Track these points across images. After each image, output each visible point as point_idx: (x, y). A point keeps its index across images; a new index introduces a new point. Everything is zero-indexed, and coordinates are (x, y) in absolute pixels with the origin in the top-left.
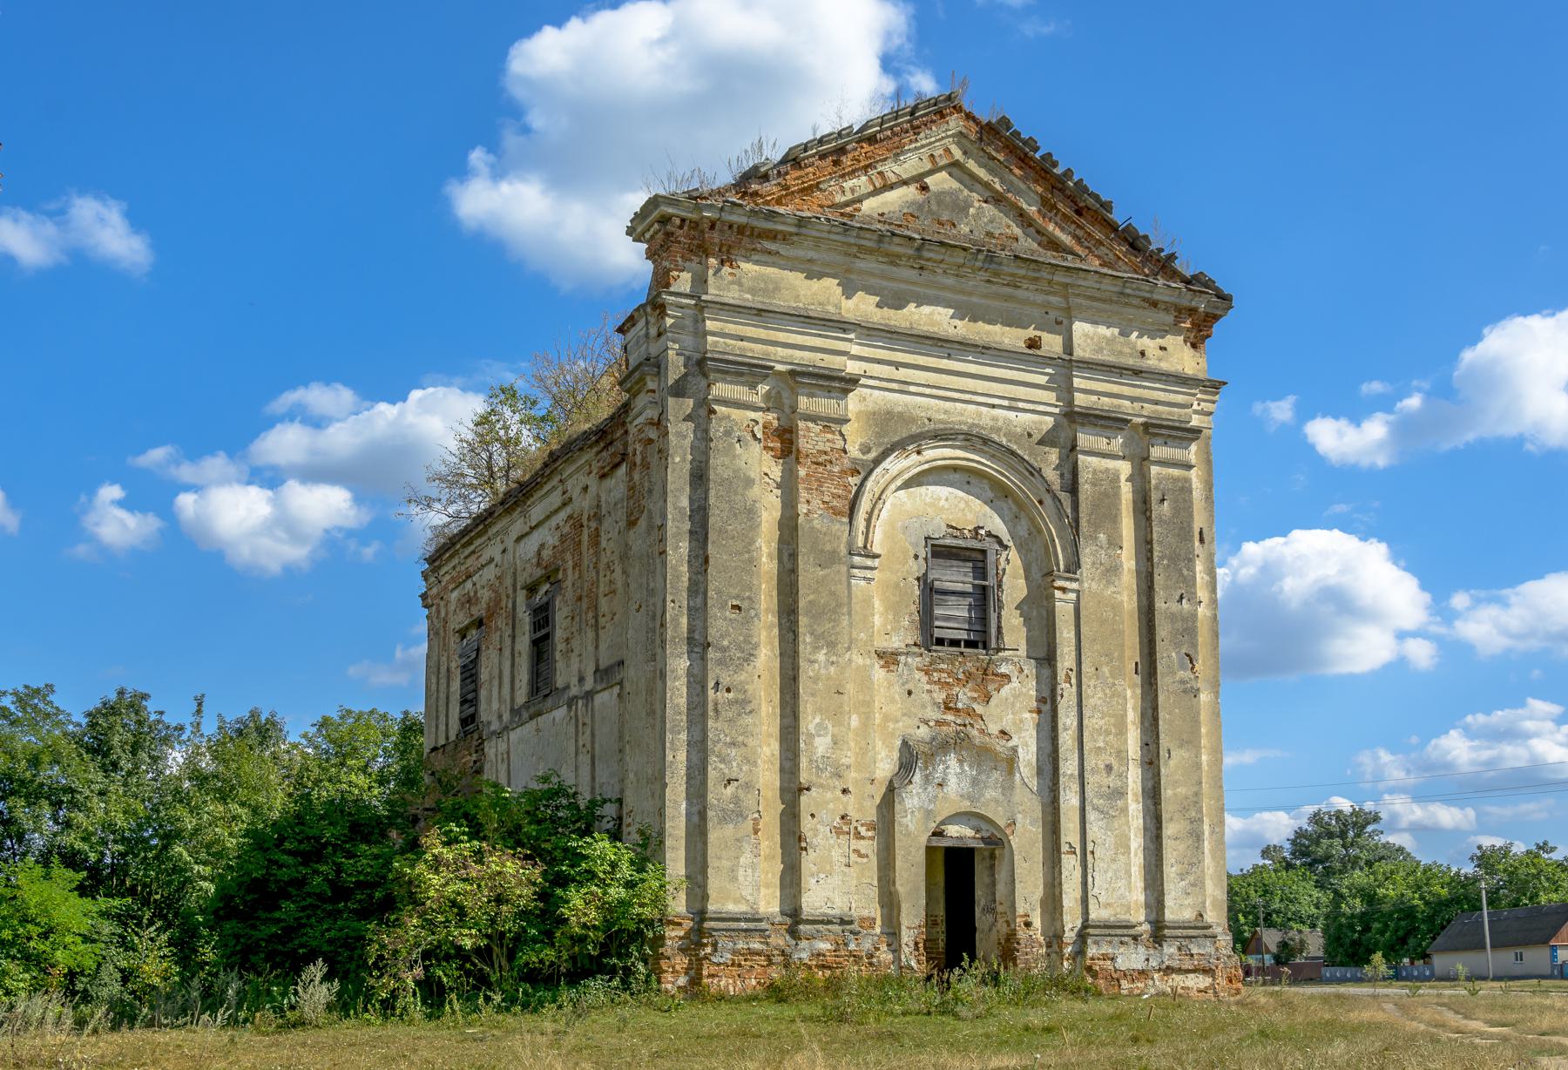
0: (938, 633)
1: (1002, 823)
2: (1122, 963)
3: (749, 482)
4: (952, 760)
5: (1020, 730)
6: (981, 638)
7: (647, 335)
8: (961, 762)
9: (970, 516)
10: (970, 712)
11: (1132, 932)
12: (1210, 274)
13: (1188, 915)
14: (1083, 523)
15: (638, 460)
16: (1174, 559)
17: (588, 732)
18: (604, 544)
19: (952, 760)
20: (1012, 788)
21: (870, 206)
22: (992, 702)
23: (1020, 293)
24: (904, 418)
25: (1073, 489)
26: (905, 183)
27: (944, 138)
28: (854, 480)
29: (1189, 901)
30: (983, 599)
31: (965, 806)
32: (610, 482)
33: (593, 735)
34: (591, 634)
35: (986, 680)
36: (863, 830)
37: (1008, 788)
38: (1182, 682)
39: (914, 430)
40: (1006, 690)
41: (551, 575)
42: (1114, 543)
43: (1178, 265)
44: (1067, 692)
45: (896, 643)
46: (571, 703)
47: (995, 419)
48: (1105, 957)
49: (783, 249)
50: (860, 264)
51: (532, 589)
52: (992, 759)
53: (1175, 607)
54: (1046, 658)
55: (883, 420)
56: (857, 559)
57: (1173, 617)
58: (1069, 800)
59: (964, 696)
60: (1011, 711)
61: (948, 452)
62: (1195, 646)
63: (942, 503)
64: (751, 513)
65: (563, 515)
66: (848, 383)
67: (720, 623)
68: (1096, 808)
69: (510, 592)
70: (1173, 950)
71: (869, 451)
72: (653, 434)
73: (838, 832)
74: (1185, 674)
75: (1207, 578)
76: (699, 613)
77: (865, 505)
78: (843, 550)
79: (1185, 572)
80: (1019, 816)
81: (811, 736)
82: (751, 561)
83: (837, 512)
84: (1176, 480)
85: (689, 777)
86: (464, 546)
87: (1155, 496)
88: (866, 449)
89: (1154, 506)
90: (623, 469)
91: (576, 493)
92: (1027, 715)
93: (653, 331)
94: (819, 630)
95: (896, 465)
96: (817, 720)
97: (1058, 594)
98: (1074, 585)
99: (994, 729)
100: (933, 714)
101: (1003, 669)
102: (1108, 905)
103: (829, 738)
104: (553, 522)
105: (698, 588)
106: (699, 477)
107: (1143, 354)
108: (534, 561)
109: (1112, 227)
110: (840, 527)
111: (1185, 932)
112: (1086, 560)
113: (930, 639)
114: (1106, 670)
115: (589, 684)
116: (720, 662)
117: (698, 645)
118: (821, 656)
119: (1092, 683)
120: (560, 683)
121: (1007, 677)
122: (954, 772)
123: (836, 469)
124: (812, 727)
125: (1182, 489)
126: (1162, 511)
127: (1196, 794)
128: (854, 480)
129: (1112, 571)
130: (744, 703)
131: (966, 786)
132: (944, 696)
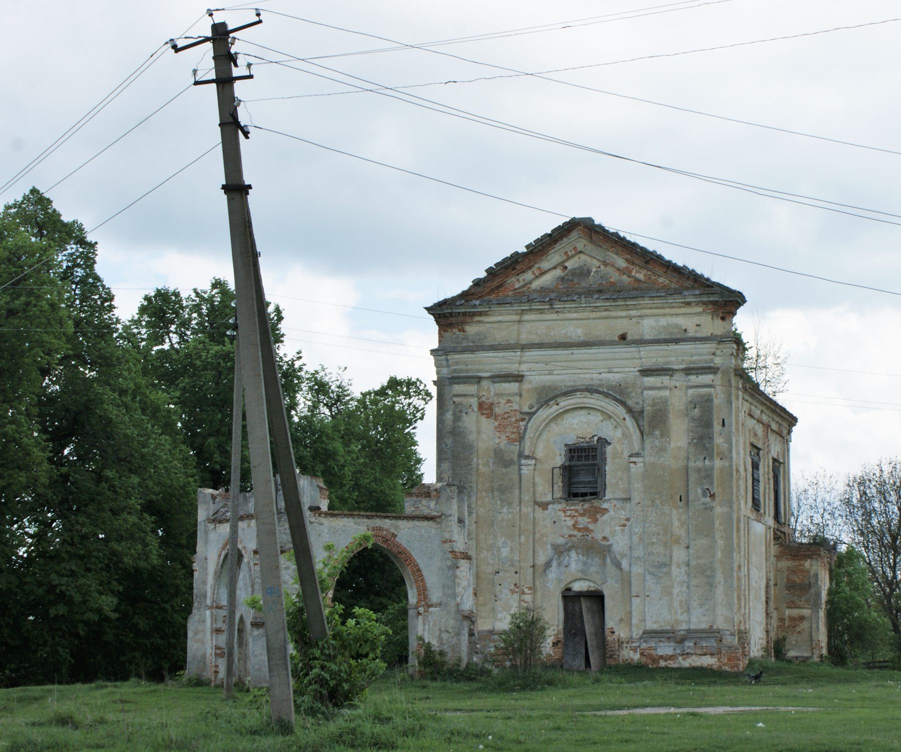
0: (574, 491)
1: (599, 583)
2: (660, 652)
4: (573, 554)
5: (614, 536)
8: (577, 553)
9: (589, 431)
10: (586, 529)
11: (667, 635)
13: (704, 626)
14: (646, 427)
19: (573, 554)
20: (604, 564)
21: (536, 284)
22: (599, 523)
23: (613, 314)
24: (551, 388)
26: (555, 268)
28: (524, 423)
29: (705, 619)
31: (580, 575)
35: (595, 514)
36: (526, 590)
38: (704, 504)
39: (557, 392)
40: (606, 517)
42: (665, 434)
45: (549, 498)
47: (601, 380)
48: (651, 648)
49: (485, 319)
50: (526, 317)
52: (597, 550)
53: (700, 464)
56: (523, 461)
57: (699, 470)
59: (583, 521)
62: (712, 484)
63: (575, 426)
66: (518, 378)
68: (650, 573)
70: (691, 644)
71: (533, 407)
73: (513, 592)
77: (529, 434)
78: (515, 458)
79: (707, 445)
80: (609, 579)
81: (499, 548)
83: (515, 440)
84: (702, 396)
88: (531, 407)
92: (618, 528)
94: (504, 498)
95: (545, 413)
96: (503, 539)
98: (641, 459)
99: (599, 536)
100: (567, 532)
101: (605, 506)
102: (655, 622)
103: (508, 549)
107: (686, 330)
110: (515, 448)
111: (699, 635)
114: (658, 502)
118: (505, 510)
119: (650, 509)
121: (606, 510)
122: (574, 561)
123: (513, 419)
124: (500, 544)
125: (707, 401)
127: (712, 563)
129: (662, 450)
131: (580, 566)
132: (573, 522)
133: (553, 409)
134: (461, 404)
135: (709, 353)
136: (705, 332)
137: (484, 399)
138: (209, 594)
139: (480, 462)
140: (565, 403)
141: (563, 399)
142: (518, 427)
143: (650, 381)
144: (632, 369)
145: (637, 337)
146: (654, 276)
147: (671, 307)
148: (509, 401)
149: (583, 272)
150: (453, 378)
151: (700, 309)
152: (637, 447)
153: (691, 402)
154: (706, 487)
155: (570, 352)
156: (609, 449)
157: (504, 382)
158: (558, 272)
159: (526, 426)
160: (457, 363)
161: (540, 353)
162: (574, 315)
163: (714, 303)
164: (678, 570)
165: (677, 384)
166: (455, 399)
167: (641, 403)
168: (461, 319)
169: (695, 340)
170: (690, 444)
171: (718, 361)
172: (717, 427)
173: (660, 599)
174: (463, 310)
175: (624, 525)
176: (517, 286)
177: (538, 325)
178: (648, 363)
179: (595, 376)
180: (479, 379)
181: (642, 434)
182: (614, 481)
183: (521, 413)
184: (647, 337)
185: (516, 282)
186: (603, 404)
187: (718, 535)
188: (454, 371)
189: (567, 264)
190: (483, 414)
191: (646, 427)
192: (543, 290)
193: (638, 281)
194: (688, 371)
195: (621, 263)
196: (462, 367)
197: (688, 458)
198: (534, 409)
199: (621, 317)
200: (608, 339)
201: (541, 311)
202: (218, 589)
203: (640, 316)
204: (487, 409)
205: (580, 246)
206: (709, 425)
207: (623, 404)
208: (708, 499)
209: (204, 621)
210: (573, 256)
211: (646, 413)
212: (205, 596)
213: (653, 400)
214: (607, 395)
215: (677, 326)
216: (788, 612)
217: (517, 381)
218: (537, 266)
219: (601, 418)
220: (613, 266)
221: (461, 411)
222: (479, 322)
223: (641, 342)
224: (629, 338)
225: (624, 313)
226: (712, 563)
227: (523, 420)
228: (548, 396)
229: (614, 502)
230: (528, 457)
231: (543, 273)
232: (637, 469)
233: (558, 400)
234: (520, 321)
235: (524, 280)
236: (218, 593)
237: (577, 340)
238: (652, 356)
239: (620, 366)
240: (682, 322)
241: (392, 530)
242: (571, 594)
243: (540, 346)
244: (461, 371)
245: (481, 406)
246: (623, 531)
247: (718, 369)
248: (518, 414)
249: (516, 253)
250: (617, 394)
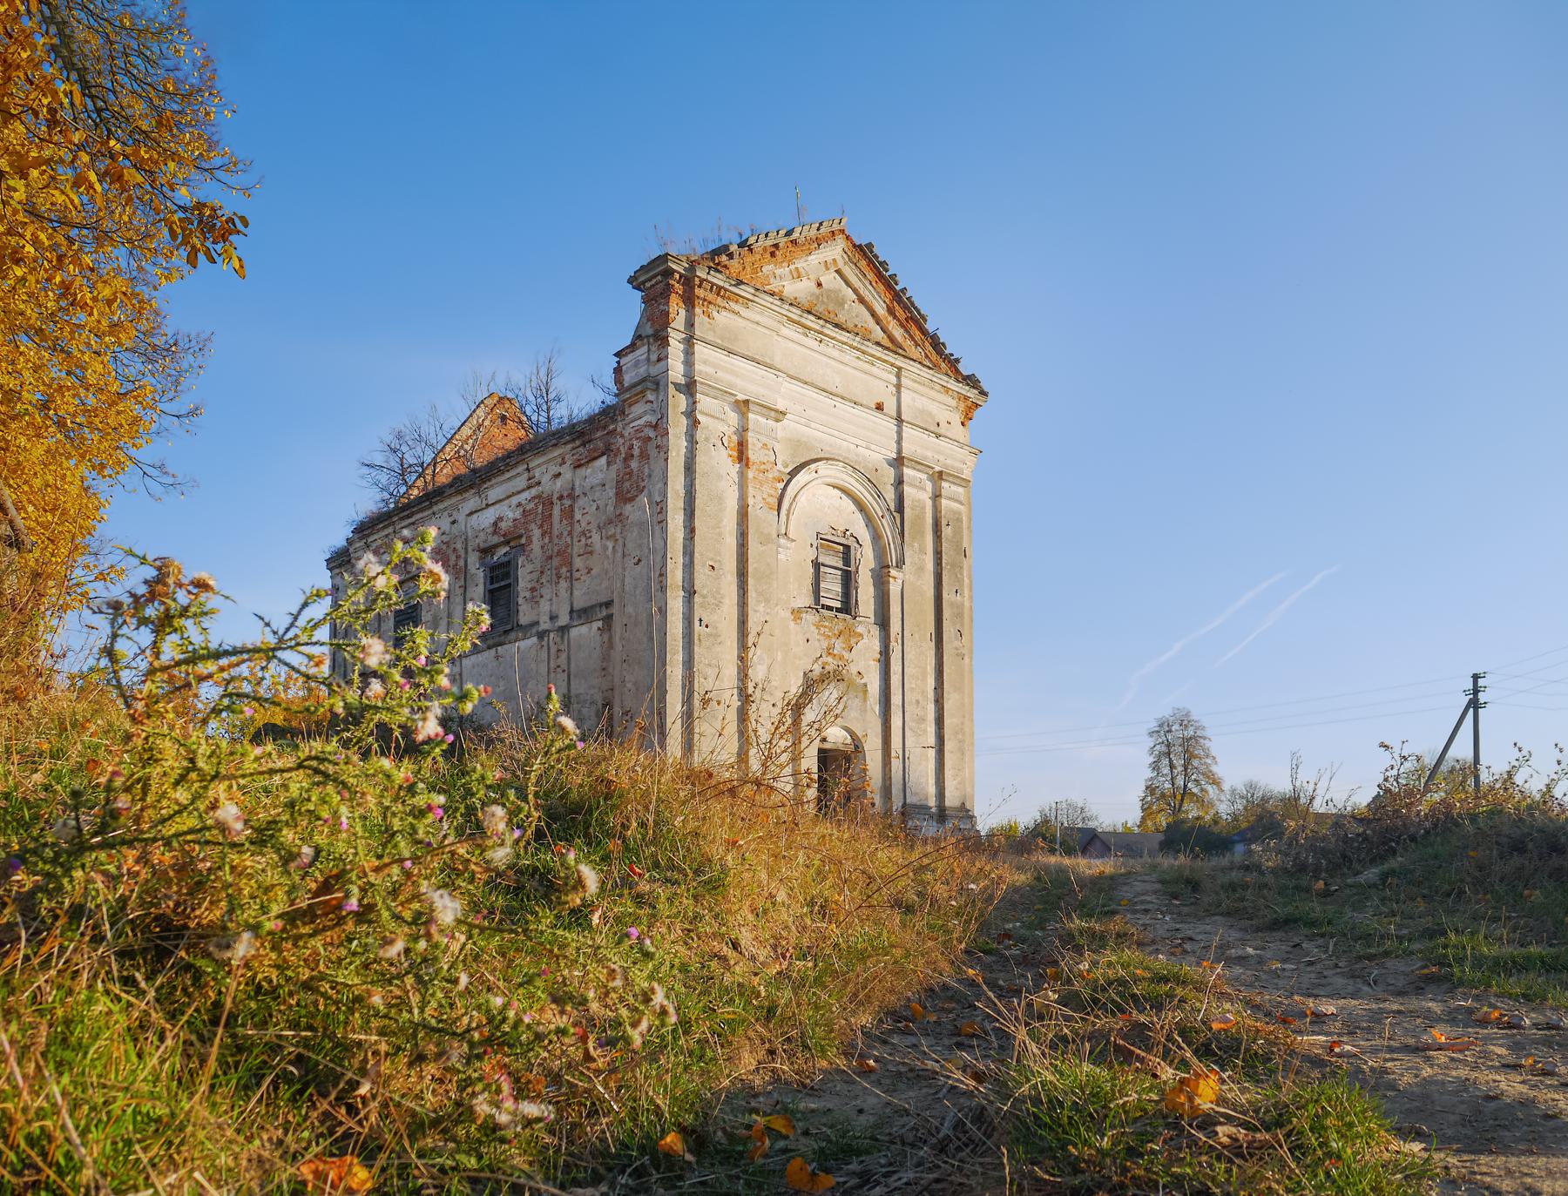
0: (823, 601)
6: (847, 606)
7: (648, 359)
12: (979, 377)
15: (636, 452)
16: (953, 565)
17: (564, 656)
18: (578, 516)
23: (874, 370)
25: (900, 508)
27: (835, 251)
30: (848, 580)
32: (582, 472)
33: (569, 658)
34: (563, 584)
35: (849, 635)
37: (864, 711)
41: (514, 539)
42: (922, 551)
43: (960, 367)
44: (895, 647)
46: (541, 635)
51: (486, 551)
54: (883, 622)
55: (797, 444)
58: (896, 722)
60: (864, 658)
64: (720, 499)
65: (526, 495)
66: (780, 415)
67: (701, 577)
69: (462, 553)
72: (652, 434)
74: (957, 644)
76: (689, 567)
82: (720, 534)
84: (955, 512)
85: (684, 687)
86: (402, 519)
87: (944, 522)
89: (944, 528)
90: (603, 460)
91: (545, 479)
93: (654, 357)
101: (860, 629)
104: (515, 500)
105: (689, 552)
106: (690, 468)
108: (490, 530)
109: (924, 332)
113: (818, 604)
115: (564, 620)
116: (702, 605)
117: (690, 592)
118: (761, 608)
120: (524, 619)
121: (861, 635)
126: (947, 532)
128: (781, 485)
130: (717, 636)
151: (954, 403)
157: (763, 415)
163: (966, 398)
168: (711, 297)
174: (721, 283)
195: (881, 310)
205: (840, 264)
215: (930, 414)
242: (827, 746)
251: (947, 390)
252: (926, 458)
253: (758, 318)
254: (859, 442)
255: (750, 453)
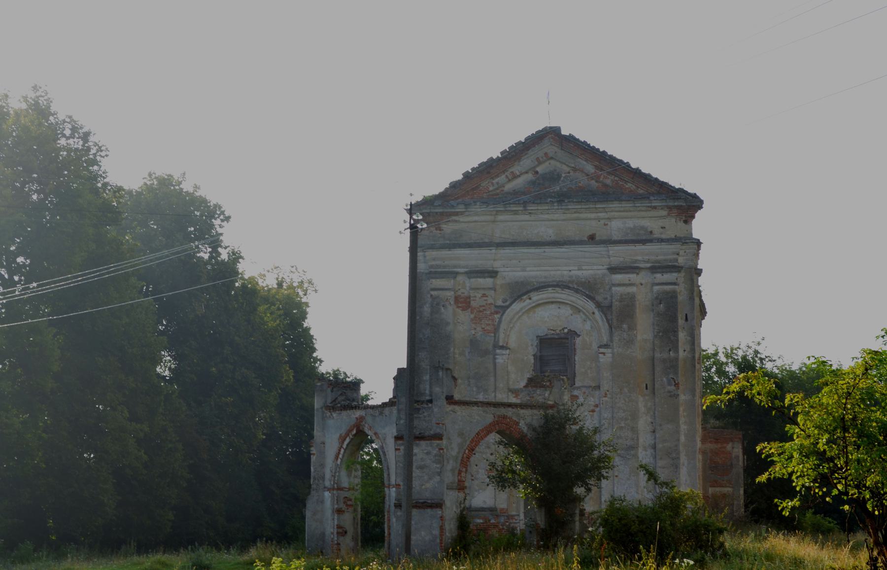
3: (448, 324)
14: (615, 321)
21: (509, 187)
26: (527, 172)
28: (497, 316)
38: (669, 392)
42: (632, 328)
47: (571, 277)
53: (665, 355)
56: (498, 351)
61: (544, 296)
62: (676, 373)
66: (493, 274)
75: (689, 338)
77: (503, 326)
78: (491, 348)
79: (672, 338)
84: (667, 293)
88: (505, 301)
95: (516, 306)
97: (601, 355)
98: (610, 350)
107: (651, 232)
112: (616, 339)
123: (488, 312)
127: (676, 446)
129: (630, 342)
133: (525, 304)
134: (438, 297)
135: (674, 253)
136: (670, 234)
137: (459, 293)
138: (328, 475)
139: (457, 351)
140: (536, 297)
141: (536, 293)
142: (493, 320)
143: (618, 277)
144: (601, 267)
145: (605, 238)
146: (619, 182)
147: (639, 211)
148: (484, 295)
149: (554, 177)
150: (430, 273)
152: (605, 339)
153: (657, 298)
154: (671, 376)
155: (542, 250)
156: (578, 341)
157: (480, 277)
158: (530, 176)
159: (500, 319)
160: (434, 259)
161: (512, 251)
162: (546, 216)
163: (679, 208)
164: (644, 453)
165: (643, 282)
166: (433, 293)
167: (609, 298)
169: (661, 241)
170: (655, 336)
171: (681, 261)
172: (681, 322)
173: (628, 479)
174: (441, 210)
175: (593, 411)
176: (491, 188)
177: (510, 224)
178: (615, 261)
179: (565, 273)
180: (455, 275)
181: (611, 327)
182: (583, 370)
183: (496, 306)
184: (615, 238)
185: (489, 185)
186: (573, 299)
187: (682, 420)
188: (432, 267)
189: (538, 169)
190: (458, 307)
191: (615, 321)
192: (515, 193)
193: (606, 185)
194: (656, 268)
195: (590, 168)
196: (438, 263)
197: (654, 350)
198: (508, 303)
199: (590, 219)
200: (577, 239)
201: (516, 213)
202: (339, 472)
203: (609, 219)
204: (464, 303)
206: (673, 319)
207: (592, 299)
208: (673, 388)
209: (322, 502)
210: (544, 162)
211: (614, 308)
212: (323, 478)
213: (621, 295)
214: (577, 291)
215: (642, 228)
216: (711, 490)
217: (491, 277)
218: (511, 170)
219: (571, 312)
220: (582, 171)
221: (438, 304)
222: (456, 221)
223: (609, 242)
224: (597, 238)
225: (593, 216)
226: (676, 446)
227: (497, 313)
228: (520, 290)
229: (584, 390)
230: (502, 347)
231: (515, 177)
232: (606, 358)
233: (532, 294)
234: (494, 221)
235: (498, 183)
236: (339, 476)
237: (548, 239)
238: (620, 254)
239: (589, 264)
240: (647, 223)
241: (514, 418)
243: (514, 244)
244: (438, 266)
245: (457, 299)
246: (592, 416)
247: (682, 267)
248: (493, 307)
249: (491, 159)
250: (587, 289)
251: (655, 208)
252: (636, 261)
253: (476, 218)
254: (571, 268)
255: (472, 302)
